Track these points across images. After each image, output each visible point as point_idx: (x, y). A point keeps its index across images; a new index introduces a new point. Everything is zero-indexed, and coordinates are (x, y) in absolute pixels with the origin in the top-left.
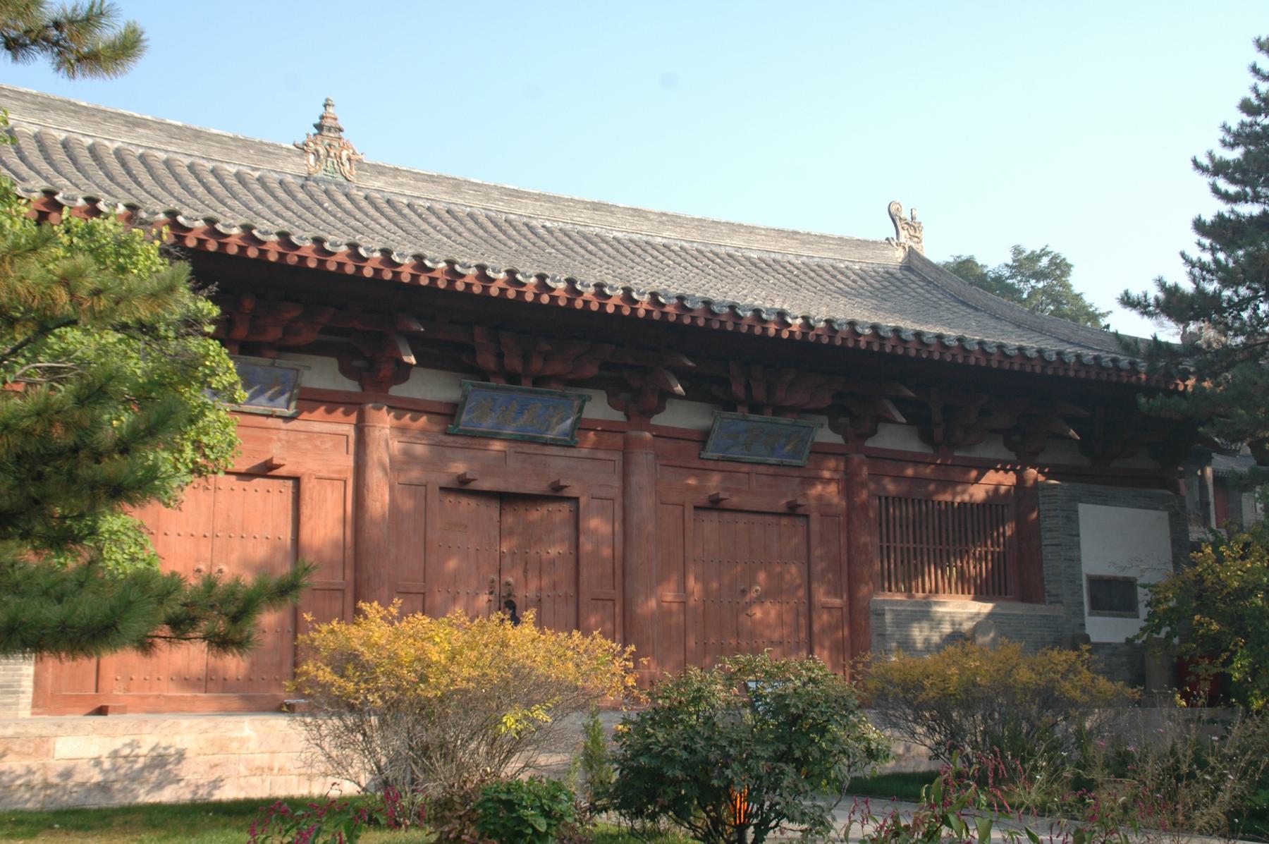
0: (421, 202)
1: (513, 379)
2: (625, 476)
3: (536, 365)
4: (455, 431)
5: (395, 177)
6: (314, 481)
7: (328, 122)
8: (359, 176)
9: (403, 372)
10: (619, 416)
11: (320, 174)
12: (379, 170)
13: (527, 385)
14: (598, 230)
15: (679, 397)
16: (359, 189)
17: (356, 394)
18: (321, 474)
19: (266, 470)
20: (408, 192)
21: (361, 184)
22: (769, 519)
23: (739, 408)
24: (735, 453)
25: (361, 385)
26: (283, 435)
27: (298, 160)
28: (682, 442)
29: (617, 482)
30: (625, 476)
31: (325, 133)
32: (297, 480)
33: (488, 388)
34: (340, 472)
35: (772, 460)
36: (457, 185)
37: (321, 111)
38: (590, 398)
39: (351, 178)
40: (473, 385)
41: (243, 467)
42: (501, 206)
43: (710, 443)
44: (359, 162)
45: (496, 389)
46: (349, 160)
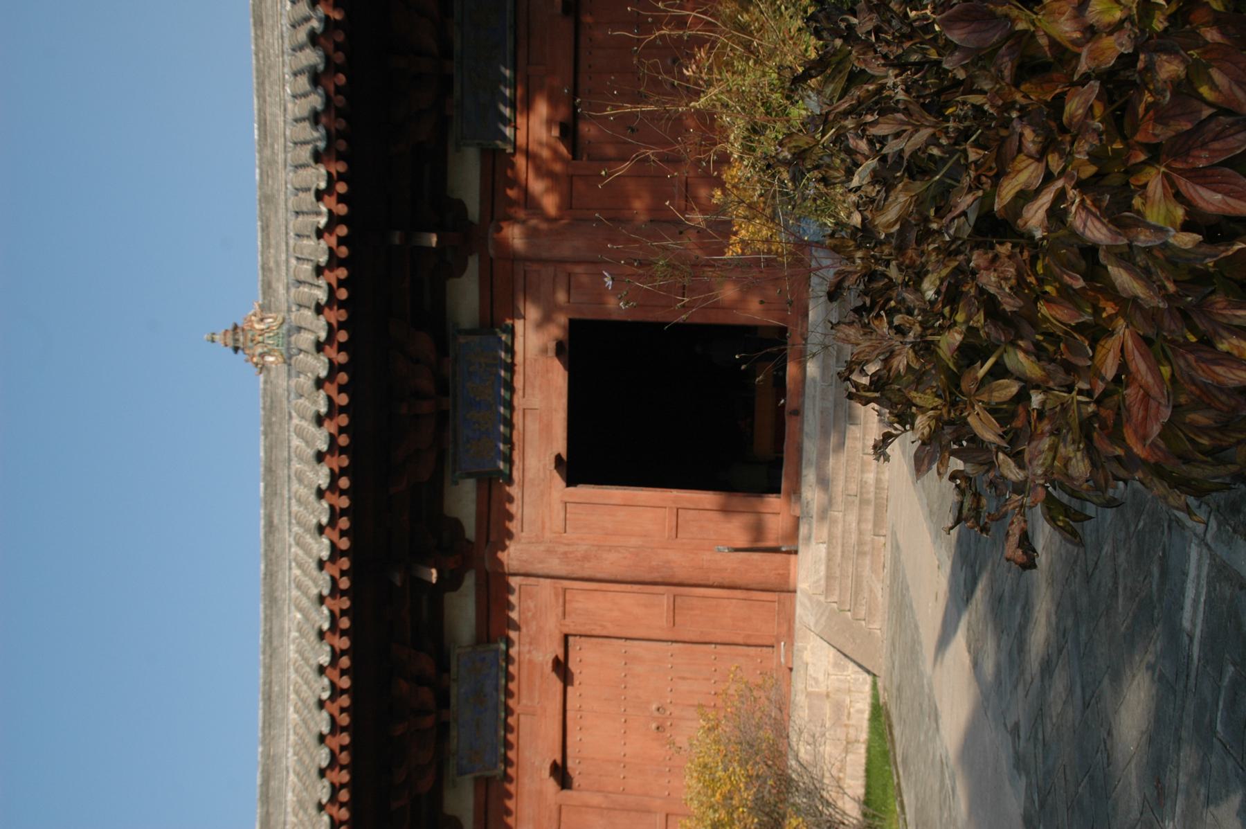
0: (292, 242)
1: (443, 418)
5: (270, 270)
6: (568, 621)
8: (278, 311)
10: (473, 264)
11: (283, 349)
12: (268, 287)
14: (285, 22)
16: (289, 310)
17: (477, 579)
18: (560, 614)
19: (562, 668)
20: (283, 257)
21: (284, 307)
26: (525, 649)
27: (273, 374)
31: (240, 345)
34: (556, 595)
35: (510, 45)
36: (267, 199)
39: (280, 319)
41: (558, 685)
42: (279, 147)
44: (262, 308)
46: (262, 320)
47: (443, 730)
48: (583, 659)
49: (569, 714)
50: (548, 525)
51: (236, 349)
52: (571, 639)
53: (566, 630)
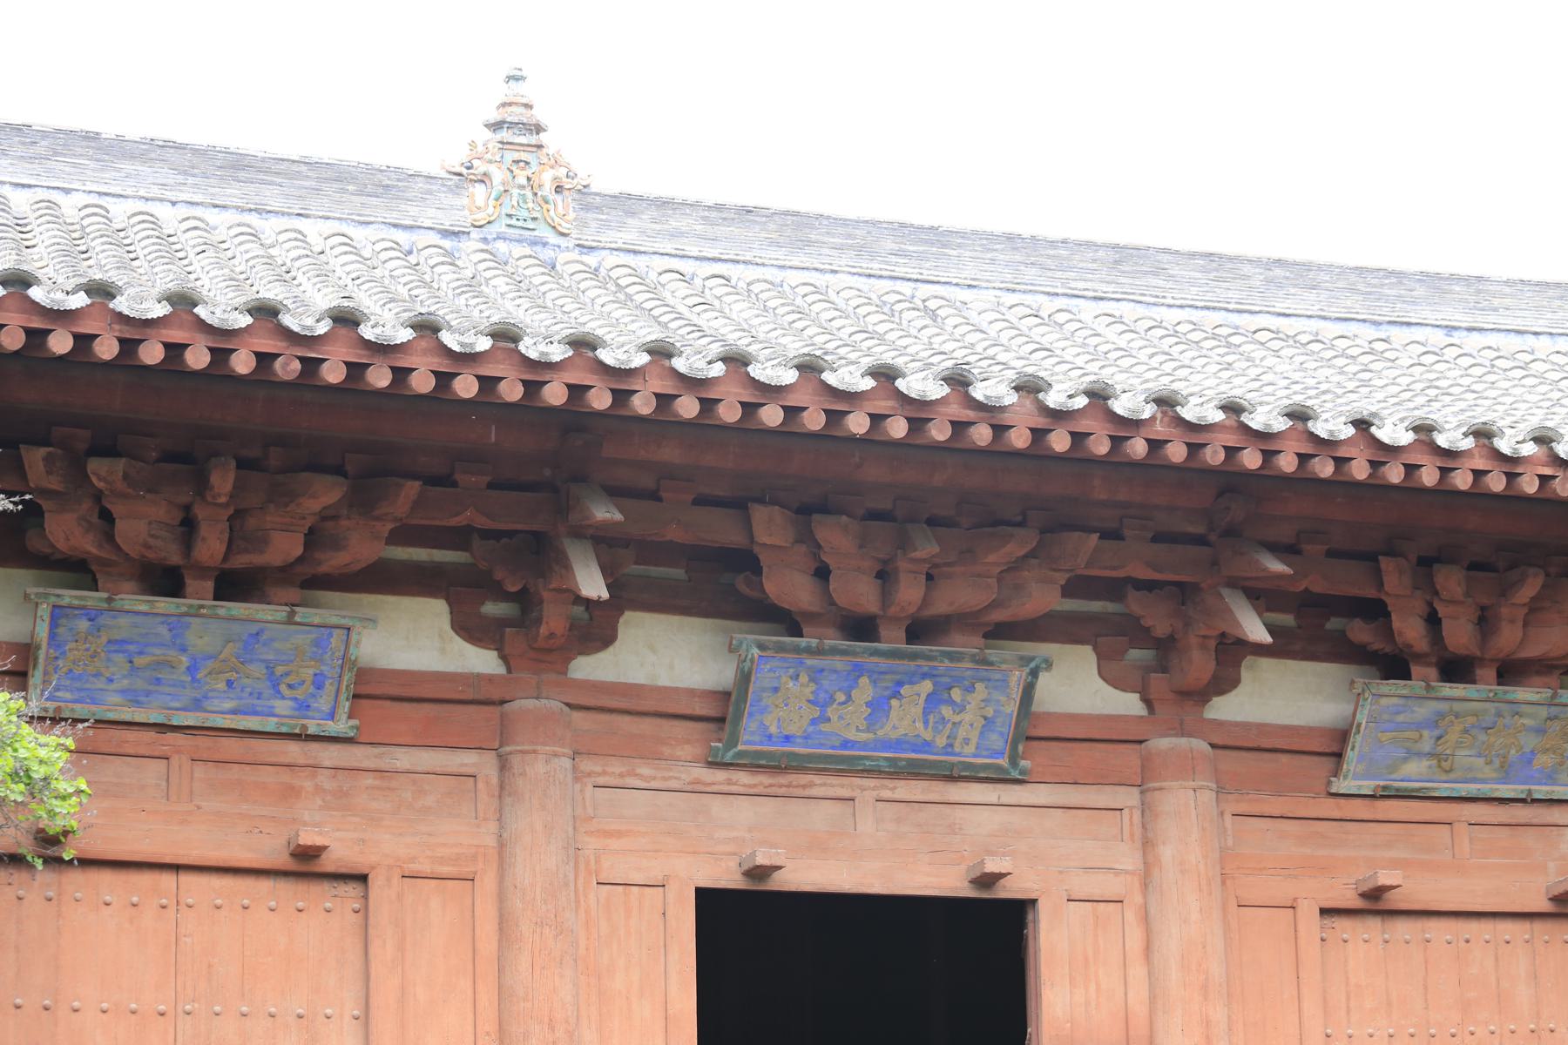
1: (861, 628)
2: (1147, 845)
3: (910, 593)
4: (728, 758)
7: (514, 114)
9: (596, 629)
10: (1129, 704)
13: (892, 638)
15: (1260, 650)
17: (490, 679)
18: (415, 867)
22: (1507, 928)
23: (1415, 670)
24: (1414, 772)
25: (504, 658)
26: (324, 779)
28: (1284, 758)
29: (1128, 859)
30: (1147, 845)
32: (362, 878)
33: (797, 650)
35: (1505, 791)
37: (504, 92)
38: (1049, 665)
40: (761, 647)
43: (1351, 755)
44: (583, 191)
45: (819, 652)
47: (165, 580)
48: (319, 916)
49: (167, 880)
50: (614, 844)
51: (496, 126)
52: (351, 890)
53: (376, 882)
